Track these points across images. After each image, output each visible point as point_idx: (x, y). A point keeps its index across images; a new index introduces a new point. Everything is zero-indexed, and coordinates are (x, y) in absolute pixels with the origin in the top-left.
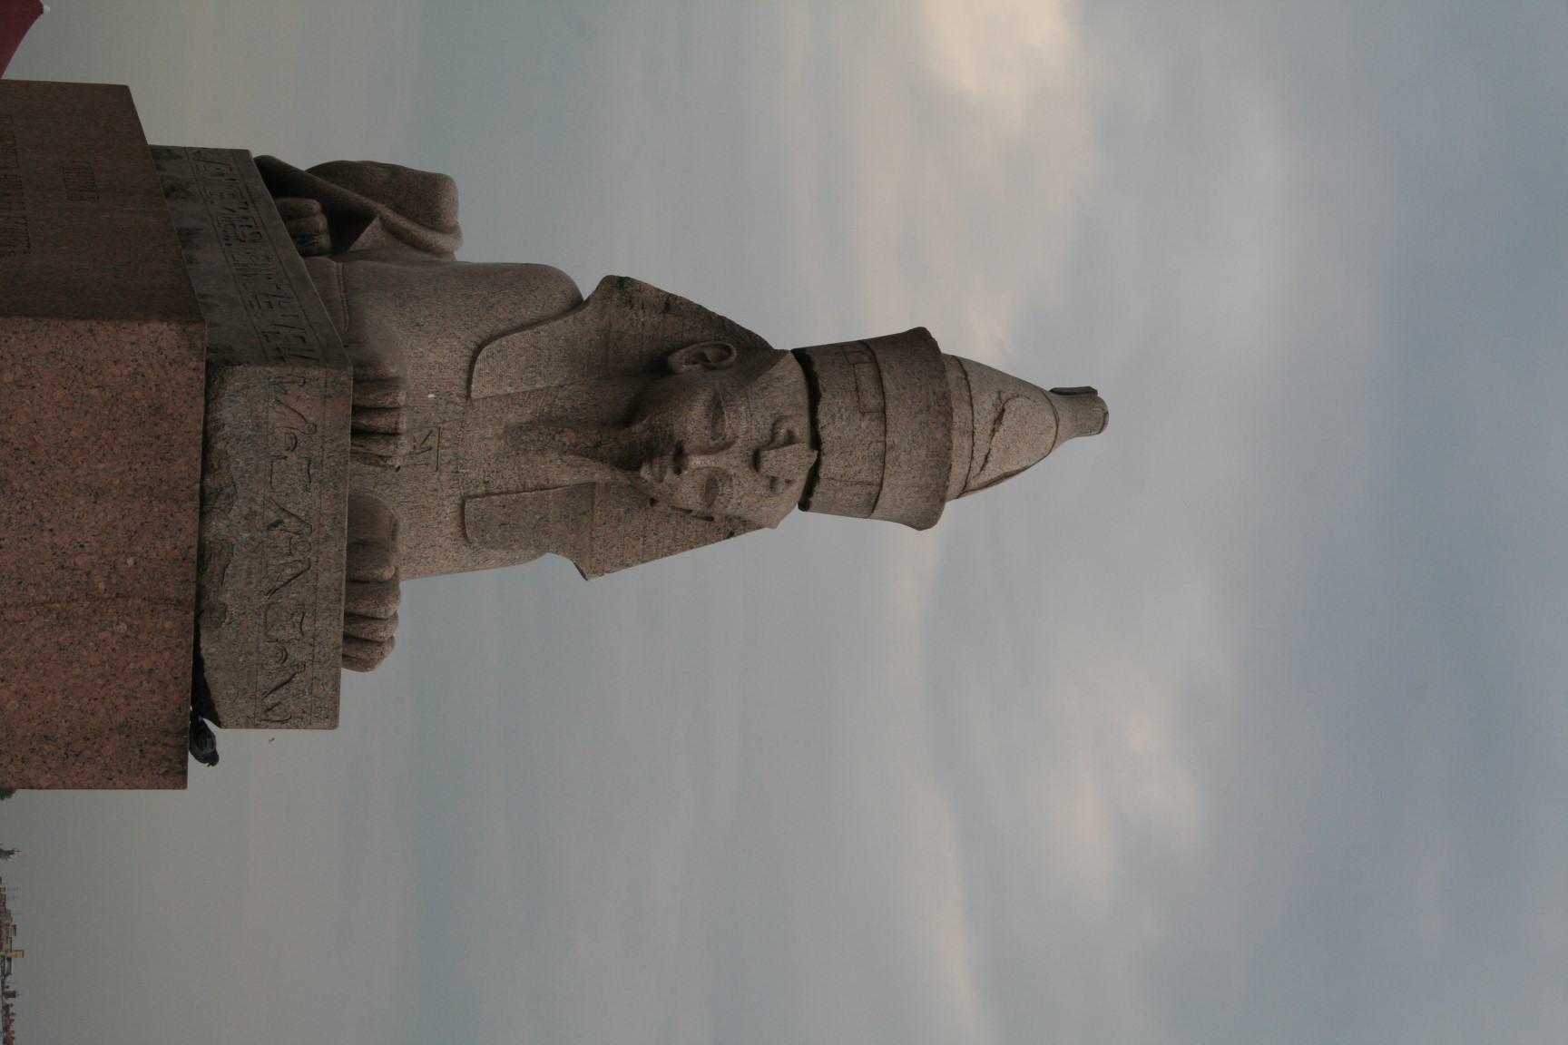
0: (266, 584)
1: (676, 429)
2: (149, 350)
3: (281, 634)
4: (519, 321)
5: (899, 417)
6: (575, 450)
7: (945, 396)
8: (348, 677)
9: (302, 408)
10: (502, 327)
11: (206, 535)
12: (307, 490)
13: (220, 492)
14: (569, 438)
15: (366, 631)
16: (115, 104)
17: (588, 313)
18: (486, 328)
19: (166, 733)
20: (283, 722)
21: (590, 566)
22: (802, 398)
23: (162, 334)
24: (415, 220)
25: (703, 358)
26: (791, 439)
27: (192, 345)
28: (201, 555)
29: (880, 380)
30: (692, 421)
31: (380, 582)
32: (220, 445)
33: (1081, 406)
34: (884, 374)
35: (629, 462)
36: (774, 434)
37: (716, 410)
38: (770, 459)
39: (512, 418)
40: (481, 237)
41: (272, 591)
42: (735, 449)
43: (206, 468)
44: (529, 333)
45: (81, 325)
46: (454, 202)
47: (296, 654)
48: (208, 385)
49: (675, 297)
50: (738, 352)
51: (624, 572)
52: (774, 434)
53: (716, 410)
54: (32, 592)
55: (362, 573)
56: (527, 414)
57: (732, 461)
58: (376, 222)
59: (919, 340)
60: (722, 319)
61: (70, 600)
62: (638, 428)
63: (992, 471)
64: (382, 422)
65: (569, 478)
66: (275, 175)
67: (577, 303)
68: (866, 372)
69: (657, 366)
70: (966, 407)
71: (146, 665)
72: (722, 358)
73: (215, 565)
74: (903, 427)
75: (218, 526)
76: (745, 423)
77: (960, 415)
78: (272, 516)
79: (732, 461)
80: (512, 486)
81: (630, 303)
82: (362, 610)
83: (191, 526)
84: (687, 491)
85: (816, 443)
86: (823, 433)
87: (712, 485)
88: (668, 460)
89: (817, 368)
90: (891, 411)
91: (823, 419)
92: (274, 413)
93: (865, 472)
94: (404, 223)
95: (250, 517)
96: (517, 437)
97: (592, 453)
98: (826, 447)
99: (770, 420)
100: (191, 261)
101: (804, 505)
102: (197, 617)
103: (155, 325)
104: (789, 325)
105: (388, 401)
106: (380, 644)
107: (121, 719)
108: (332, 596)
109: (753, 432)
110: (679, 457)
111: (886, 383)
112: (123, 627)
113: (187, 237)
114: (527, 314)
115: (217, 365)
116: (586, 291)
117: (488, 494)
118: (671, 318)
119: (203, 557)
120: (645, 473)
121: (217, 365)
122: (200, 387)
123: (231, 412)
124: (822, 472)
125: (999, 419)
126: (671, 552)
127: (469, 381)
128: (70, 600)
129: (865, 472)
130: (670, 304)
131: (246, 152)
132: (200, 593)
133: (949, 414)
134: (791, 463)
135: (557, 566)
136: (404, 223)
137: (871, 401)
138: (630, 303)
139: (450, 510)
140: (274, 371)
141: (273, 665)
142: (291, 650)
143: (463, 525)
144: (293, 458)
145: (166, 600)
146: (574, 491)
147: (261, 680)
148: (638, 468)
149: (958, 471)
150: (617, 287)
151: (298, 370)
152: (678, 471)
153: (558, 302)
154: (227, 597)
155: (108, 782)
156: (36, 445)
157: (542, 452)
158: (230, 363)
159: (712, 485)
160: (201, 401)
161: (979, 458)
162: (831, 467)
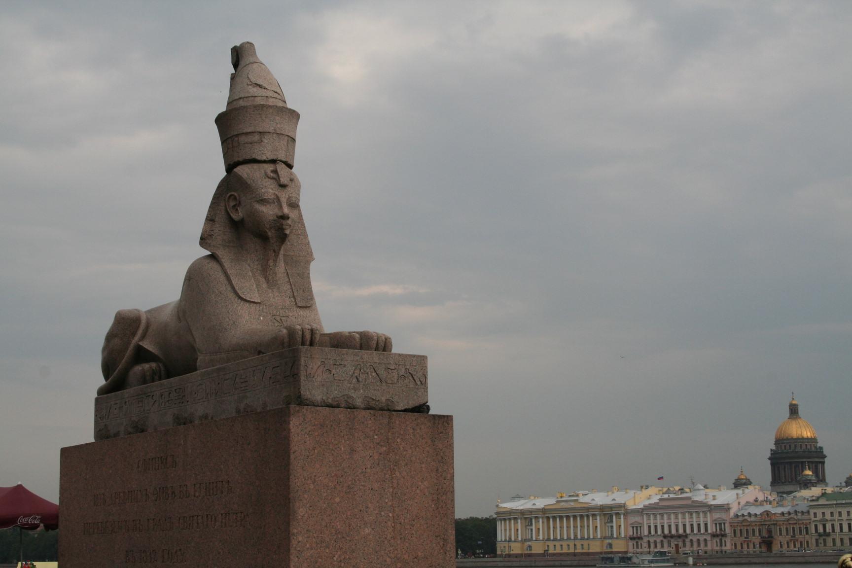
0: (379, 383)
1: (271, 218)
2: (300, 429)
3: (396, 377)
4: (226, 282)
5: (251, 128)
6: (275, 261)
7: (256, 107)
8: (395, 350)
9: (315, 367)
10: (229, 288)
11: (362, 406)
12: (345, 366)
13: (347, 402)
14: (271, 263)
15: (382, 344)
17: (220, 253)
18: (231, 295)
19: (434, 423)
20: (426, 378)
22: (256, 166)
23: (294, 423)
24: (138, 327)
25: (234, 206)
26: (275, 171)
27: (298, 411)
28: (368, 409)
29: (247, 134)
30: (268, 212)
31: (361, 338)
32: (330, 401)
34: (245, 131)
36: (273, 178)
37: (263, 201)
38: (284, 180)
39: (264, 286)
41: (381, 381)
42: (279, 195)
43: (338, 406)
44: (232, 278)
45: (292, 456)
46: (130, 311)
47: (402, 372)
48: (308, 405)
49: (207, 217)
50: (230, 191)
51: (311, 244)
52: (273, 178)
53: (263, 201)
54: (387, 476)
55: (358, 345)
56: (262, 280)
58: (141, 343)
60: (214, 198)
61: (389, 461)
62: (270, 234)
63: (278, 91)
64: (308, 336)
67: (213, 257)
68: (243, 139)
69: (236, 226)
70: (256, 99)
71: (411, 431)
72: (235, 198)
73: (372, 403)
74: (268, 124)
75: (359, 402)
77: (259, 101)
78: (355, 380)
79: (284, 196)
80: (289, 287)
81: (211, 236)
82: (375, 346)
83: (363, 412)
84: (293, 215)
85: (273, 161)
86: (270, 158)
88: (284, 222)
89: (241, 159)
90: (261, 130)
91: (264, 158)
92: (318, 379)
93: (284, 142)
94: (140, 332)
95: (355, 389)
96: (272, 283)
97: (276, 253)
98: (275, 158)
99: (267, 179)
100: (205, 417)
101: (290, 167)
102: (389, 410)
103: (291, 426)
105: (300, 333)
106: (386, 339)
107: (430, 441)
108: (382, 357)
109: (272, 186)
110: (284, 217)
111: (249, 130)
112: (399, 440)
113: (182, 421)
114: (222, 278)
115: (302, 402)
117: (294, 297)
118: (217, 219)
119: (369, 408)
120: (288, 232)
122: (313, 409)
123: (318, 395)
124: (284, 160)
125: (260, 86)
126: (303, 224)
127: (254, 302)
128: (389, 461)
129: (284, 142)
131: (97, 399)
132: (382, 409)
133: (263, 106)
136: (140, 332)
137: (256, 137)
138: (211, 236)
139: (302, 312)
140: (302, 378)
141: (406, 381)
142: (401, 374)
143: (306, 307)
144: (333, 371)
145: (389, 423)
146: (286, 263)
147: (412, 386)
148: (286, 235)
149: (280, 104)
150: (204, 241)
151: (302, 368)
152: (288, 218)
153: (213, 265)
154: (384, 399)
155: (451, 446)
156: (336, 475)
157: (275, 273)
158: (300, 397)
160: (318, 408)
161: (276, 95)
162: (281, 156)
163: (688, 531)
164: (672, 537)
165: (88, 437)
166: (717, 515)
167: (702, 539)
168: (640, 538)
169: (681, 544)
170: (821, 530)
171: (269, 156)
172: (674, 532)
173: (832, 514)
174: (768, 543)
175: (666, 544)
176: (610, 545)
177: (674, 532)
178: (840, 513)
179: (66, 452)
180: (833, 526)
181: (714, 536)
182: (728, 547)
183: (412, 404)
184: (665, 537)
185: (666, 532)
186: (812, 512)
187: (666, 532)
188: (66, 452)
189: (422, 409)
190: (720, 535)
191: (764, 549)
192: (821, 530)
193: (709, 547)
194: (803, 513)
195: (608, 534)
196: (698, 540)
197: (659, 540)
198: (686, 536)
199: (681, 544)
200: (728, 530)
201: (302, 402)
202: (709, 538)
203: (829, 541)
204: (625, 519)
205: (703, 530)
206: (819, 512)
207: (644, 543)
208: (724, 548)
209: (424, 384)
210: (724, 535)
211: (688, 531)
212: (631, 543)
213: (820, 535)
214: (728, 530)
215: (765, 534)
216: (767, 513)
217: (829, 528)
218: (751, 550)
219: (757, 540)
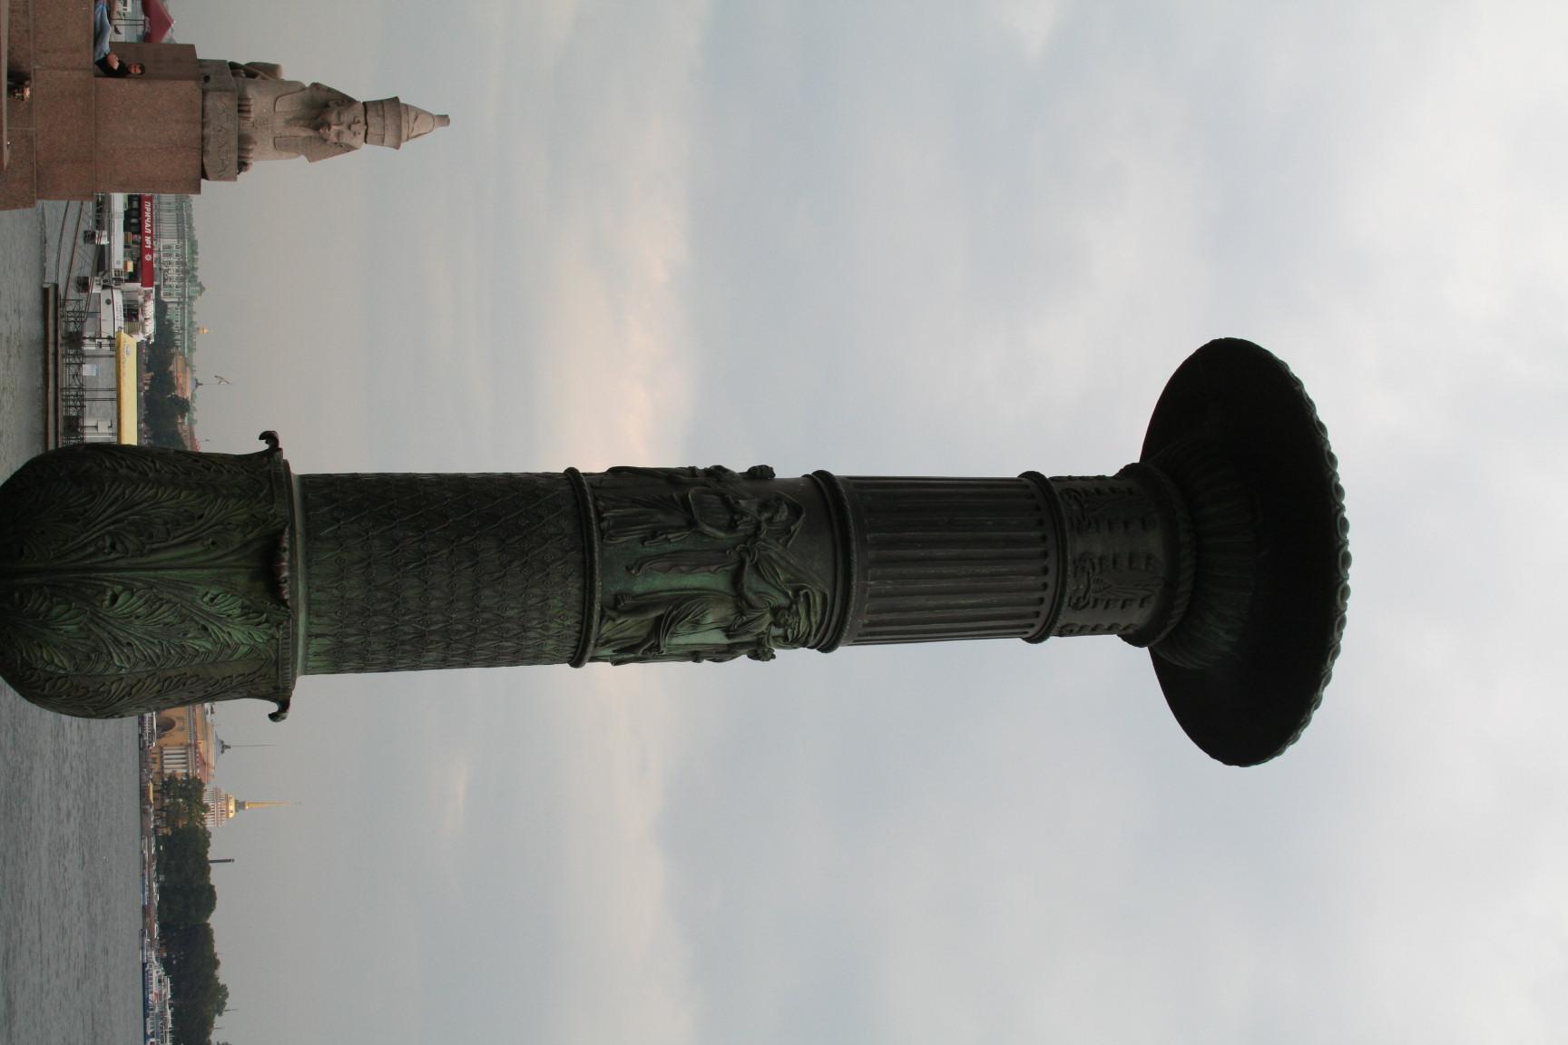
16: (191, 48)
21: (312, 159)
30: (333, 117)
33: (444, 119)
35: (317, 128)
37: (339, 115)
50: (346, 101)
53: (339, 115)
59: (396, 99)
66: (234, 66)
69: (326, 105)
75: (206, 131)
76: (347, 118)
77: (404, 117)
87: (339, 134)
96: (289, 123)
97: (308, 126)
104: (361, 94)
116: (307, 85)
123: (209, 103)
129: (379, 131)
130: (329, 90)
134: (360, 128)
135: (303, 158)
149: (404, 132)
150: (316, 86)
159: (339, 134)
162: (371, 130)
183: (207, 168)
189: (204, 176)
201: (204, 93)
209: (220, 178)
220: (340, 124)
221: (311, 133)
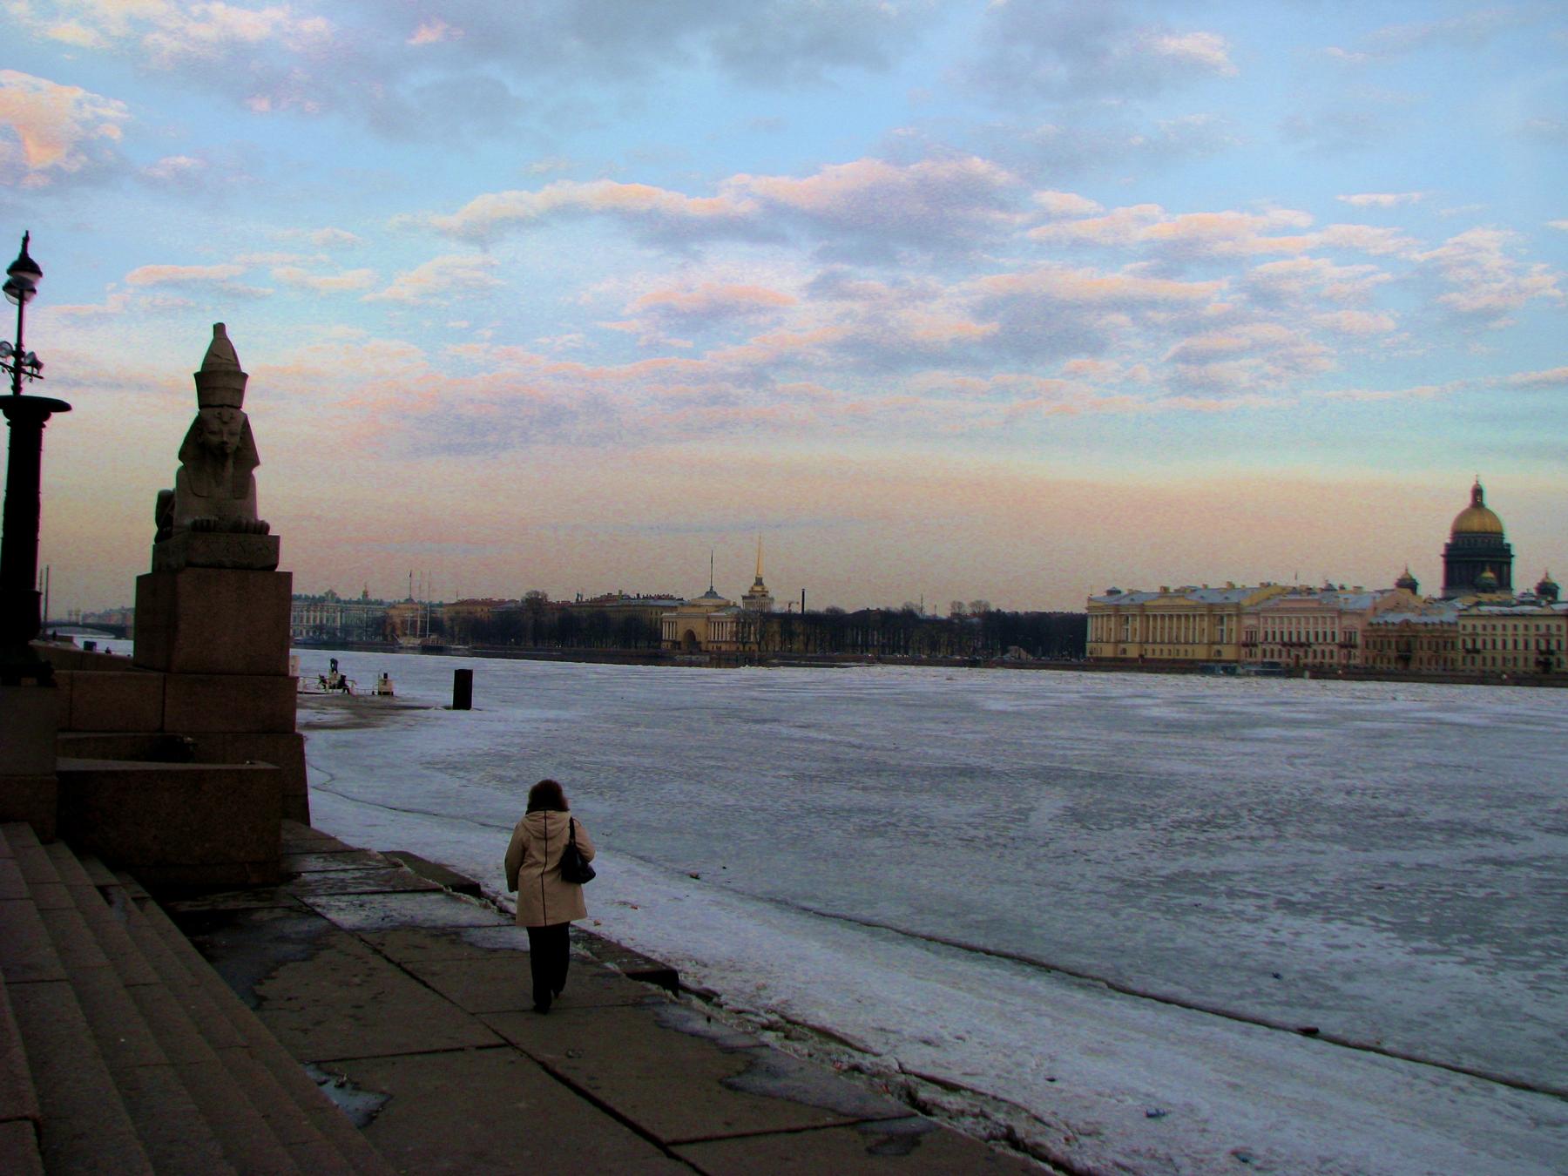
16: (142, 581)
30: (215, 439)
33: (219, 329)
35: (225, 456)
37: (213, 433)
40: (171, 485)
50: (198, 427)
53: (213, 433)
57: (225, 429)
65: (231, 470)
76: (215, 425)
79: (225, 429)
84: (235, 441)
110: (225, 443)
116: (181, 464)
121: (190, 564)
134: (227, 413)
135: (256, 472)
149: (232, 368)
150: (182, 456)
159: (232, 434)
162: (228, 402)
163: (1312, 639)
164: (1292, 645)
165: (149, 571)
166: (1346, 622)
167: (1327, 649)
168: (1255, 645)
169: (1302, 654)
170: (1469, 646)
171: (218, 402)
172: (1294, 639)
173: (1484, 628)
174: (1405, 659)
175: (1284, 654)
176: (1219, 652)
177: (1294, 639)
178: (1494, 628)
179: (139, 578)
180: (1484, 642)
181: (1342, 646)
182: (1357, 661)
184: (1284, 645)
185: (1286, 639)
186: (1461, 622)
187: (1286, 639)
188: (139, 578)
190: (1348, 645)
191: (1400, 666)
192: (1469, 646)
193: (1336, 660)
194: (1449, 624)
195: (1218, 638)
196: (1323, 652)
197: (1276, 648)
198: (1309, 645)
199: (1302, 654)
200: (1359, 640)
202: (1335, 649)
203: (1478, 658)
204: (1239, 622)
205: (1329, 640)
206: (1469, 623)
207: (1259, 651)
208: (1352, 662)
210: (1354, 646)
211: (1312, 639)
212: (1244, 651)
213: (1468, 651)
214: (1359, 640)
215: (1402, 647)
216: (1407, 622)
217: (1479, 645)
218: (1385, 666)
219: (1393, 654)
220: (221, 433)
221: (230, 463)
